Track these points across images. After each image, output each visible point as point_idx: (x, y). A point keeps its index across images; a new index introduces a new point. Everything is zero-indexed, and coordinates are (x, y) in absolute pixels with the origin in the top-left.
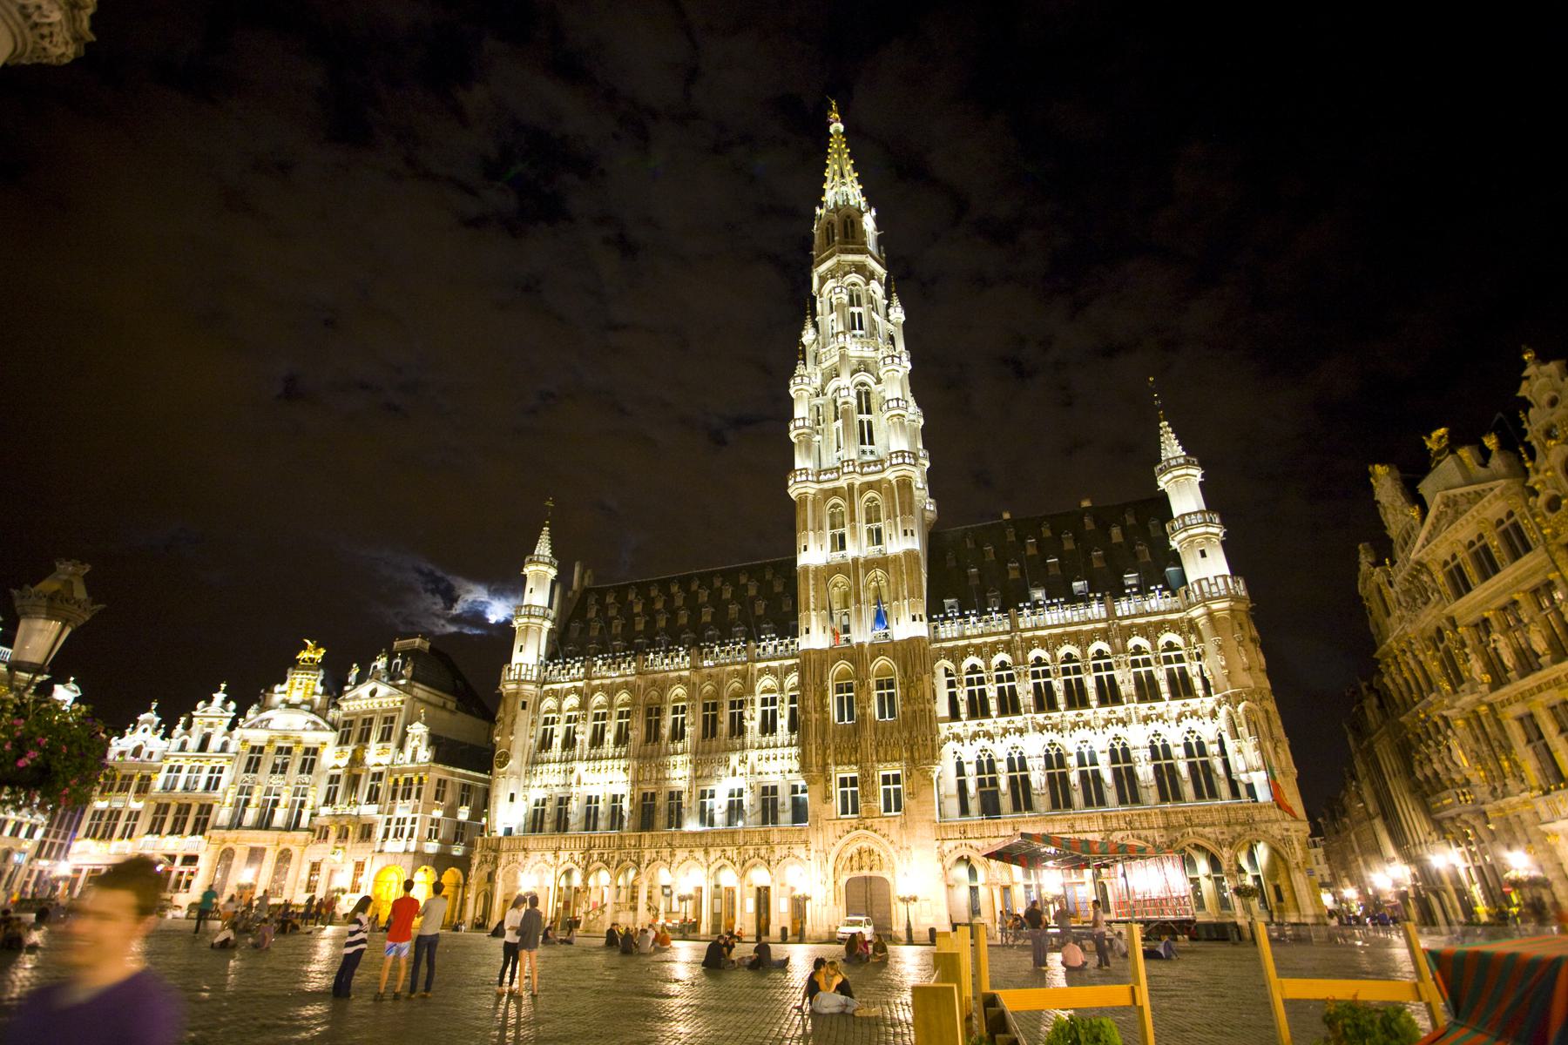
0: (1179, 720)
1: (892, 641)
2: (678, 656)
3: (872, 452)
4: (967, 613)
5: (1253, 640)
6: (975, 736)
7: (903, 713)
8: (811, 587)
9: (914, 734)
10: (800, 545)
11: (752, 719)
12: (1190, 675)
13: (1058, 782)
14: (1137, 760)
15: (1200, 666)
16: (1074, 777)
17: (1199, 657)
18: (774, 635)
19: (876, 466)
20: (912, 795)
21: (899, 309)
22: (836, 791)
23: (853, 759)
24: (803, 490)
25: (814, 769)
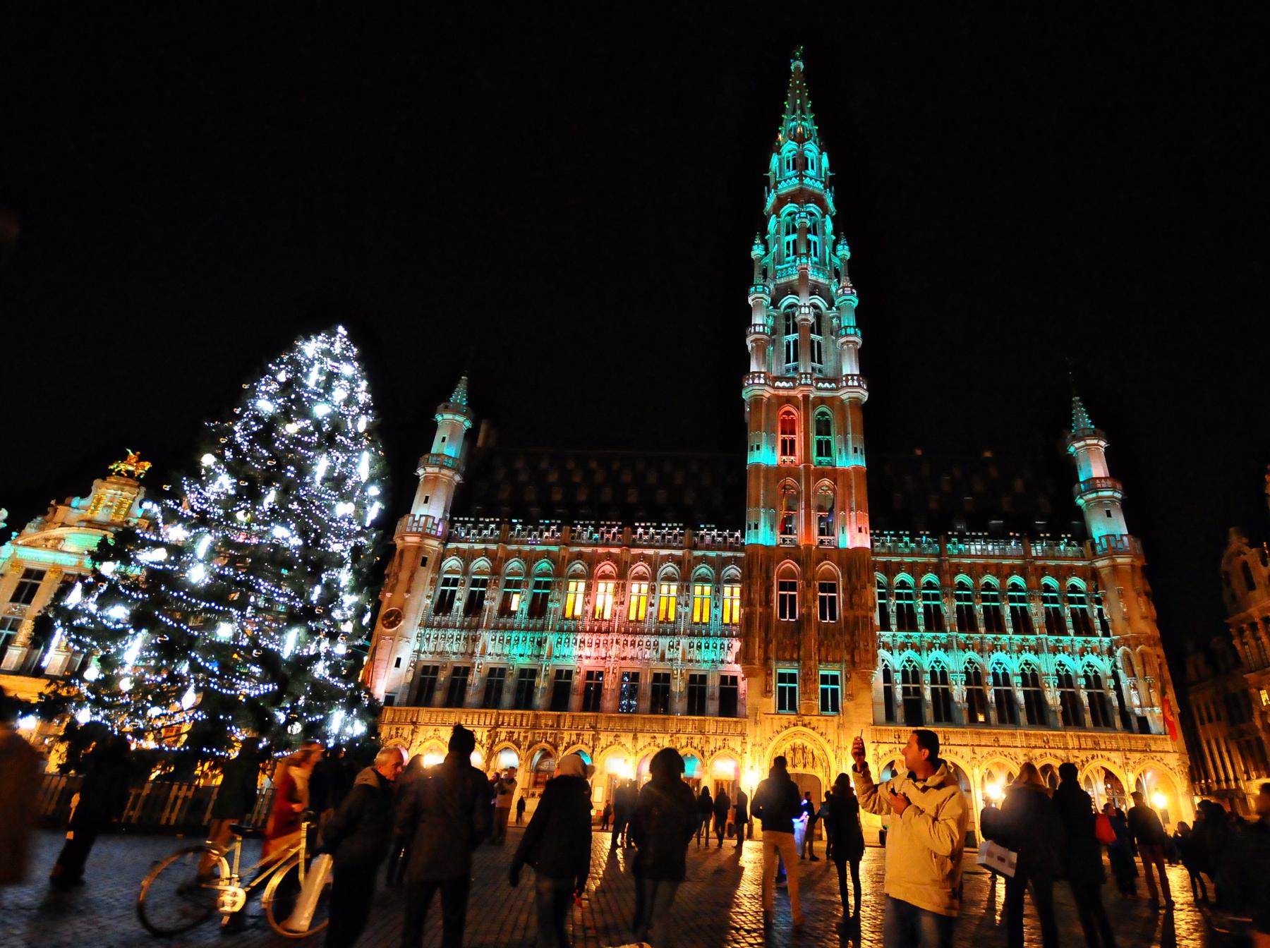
0: (1082, 655)
1: (837, 548)
2: (609, 532)
3: (820, 371)
4: (901, 532)
5: (1147, 594)
6: (903, 647)
7: (845, 617)
8: (762, 485)
9: (856, 638)
10: (752, 441)
11: (687, 605)
12: (1090, 615)
13: (976, 700)
14: (1047, 685)
15: (1100, 611)
16: (991, 696)
17: (1099, 601)
18: (713, 526)
19: (830, 384)
20: (851, 697)
21: (847, 247)
22: (775, 685)
23: (795, 656)
24: (760, 393)
25: (757, 662)
